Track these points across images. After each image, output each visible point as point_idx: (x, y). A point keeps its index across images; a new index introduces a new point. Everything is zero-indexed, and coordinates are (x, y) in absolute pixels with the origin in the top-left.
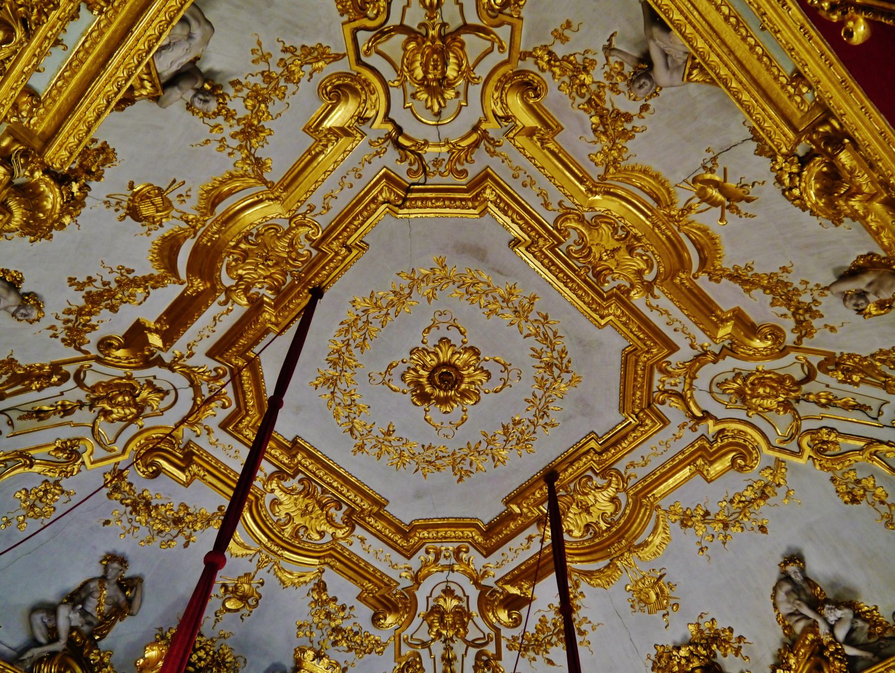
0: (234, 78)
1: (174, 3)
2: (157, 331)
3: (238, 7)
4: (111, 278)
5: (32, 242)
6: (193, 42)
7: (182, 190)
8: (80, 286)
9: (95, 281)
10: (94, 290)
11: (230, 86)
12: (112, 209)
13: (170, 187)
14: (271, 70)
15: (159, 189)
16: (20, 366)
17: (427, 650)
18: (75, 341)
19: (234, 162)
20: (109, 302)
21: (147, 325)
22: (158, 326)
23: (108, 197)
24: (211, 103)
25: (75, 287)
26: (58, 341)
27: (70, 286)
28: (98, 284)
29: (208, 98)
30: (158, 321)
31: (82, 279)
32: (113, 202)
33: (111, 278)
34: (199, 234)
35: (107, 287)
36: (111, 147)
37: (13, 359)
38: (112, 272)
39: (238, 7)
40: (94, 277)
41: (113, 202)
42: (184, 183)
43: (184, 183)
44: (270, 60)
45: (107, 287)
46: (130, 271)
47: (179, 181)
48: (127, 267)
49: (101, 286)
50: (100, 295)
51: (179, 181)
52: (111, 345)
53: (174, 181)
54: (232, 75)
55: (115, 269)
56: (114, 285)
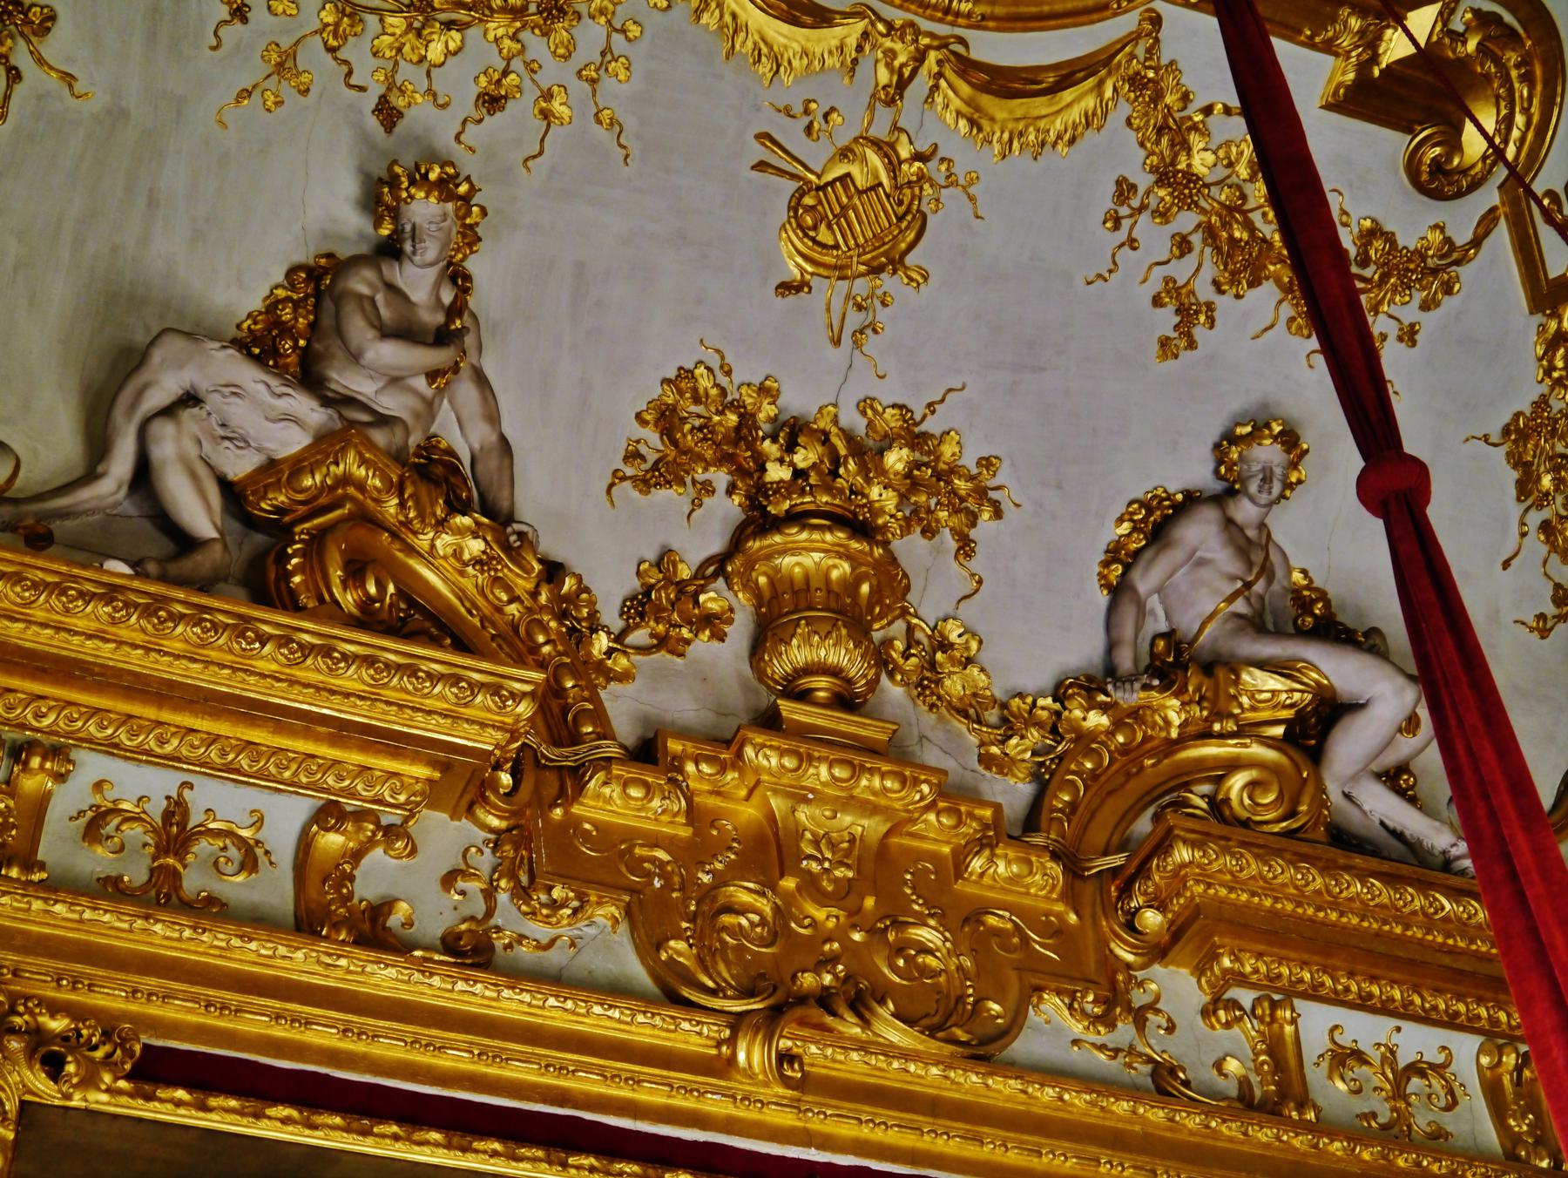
0: (373, 124)
1: (10, 594)
2: (1371, 42)
3: (152, 203)
4: (1154, 237)
5: (998, 514)
6: (203, 385)
7: (791, 134)
8: (1190, 314)
9: (1168, 280)
10: (1209, 271)
11: (401, 126)
12: (882, 315)
13: (781, 172)
14: (317, 25)
15: (795, 206)
16: (1542, 403)
17: (1134, 235)
18: (1435, 271)
19: (657, 15)
20: (1256, 217)
21: (1351, 76)
22: (1346, 42)
23: (837, 342)
24: (418, 220)
25: (1199, 333)
26: (1429, 322)
27: (1192, 345)
28: (1181, 270)
29: (408, 228)
30: (1329, 47)
31: (1167, 319)
32: (855, 319)
33: (1154, 237)
34: (943, 30)
35: (1196, 239)
36: (657, 391)
37: (1506, 431)
38: (1132, 243)
39: (152, 203)
40: (1155, 285)
41: (855, 319)
42: (764, 137)
43: (764, 137)
44: (286, 43)
45: (1196, 239)
46: (1124, 189)
47: (760, 152)
48: (1107, 203)
49: (1190, 261)
50: (1227, 251)
51: (760, 152)
52: (1437, 167)
53: (761, 166)
54: (364, 137)
55: (1122, 235)
56: (1186, 221)
